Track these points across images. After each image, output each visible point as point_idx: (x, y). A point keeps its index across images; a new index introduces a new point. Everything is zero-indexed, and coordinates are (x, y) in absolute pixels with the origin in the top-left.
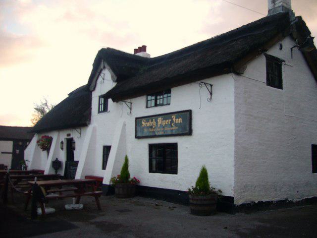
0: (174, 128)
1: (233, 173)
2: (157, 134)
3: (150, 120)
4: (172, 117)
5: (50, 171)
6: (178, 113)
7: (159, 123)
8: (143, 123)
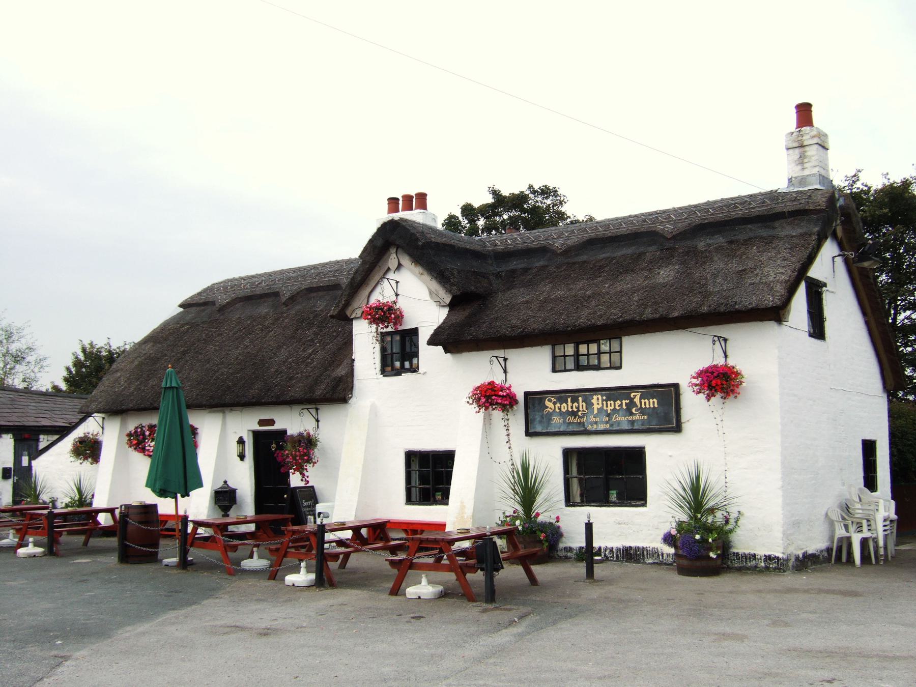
0: (637, 417)
1: (780, 501)
2: (589, 428)
3: (569, 400)
4: (632, 395)
5: (208, 516)
6: (648, 390)
7: (596, 407)
8: (547, 403)
